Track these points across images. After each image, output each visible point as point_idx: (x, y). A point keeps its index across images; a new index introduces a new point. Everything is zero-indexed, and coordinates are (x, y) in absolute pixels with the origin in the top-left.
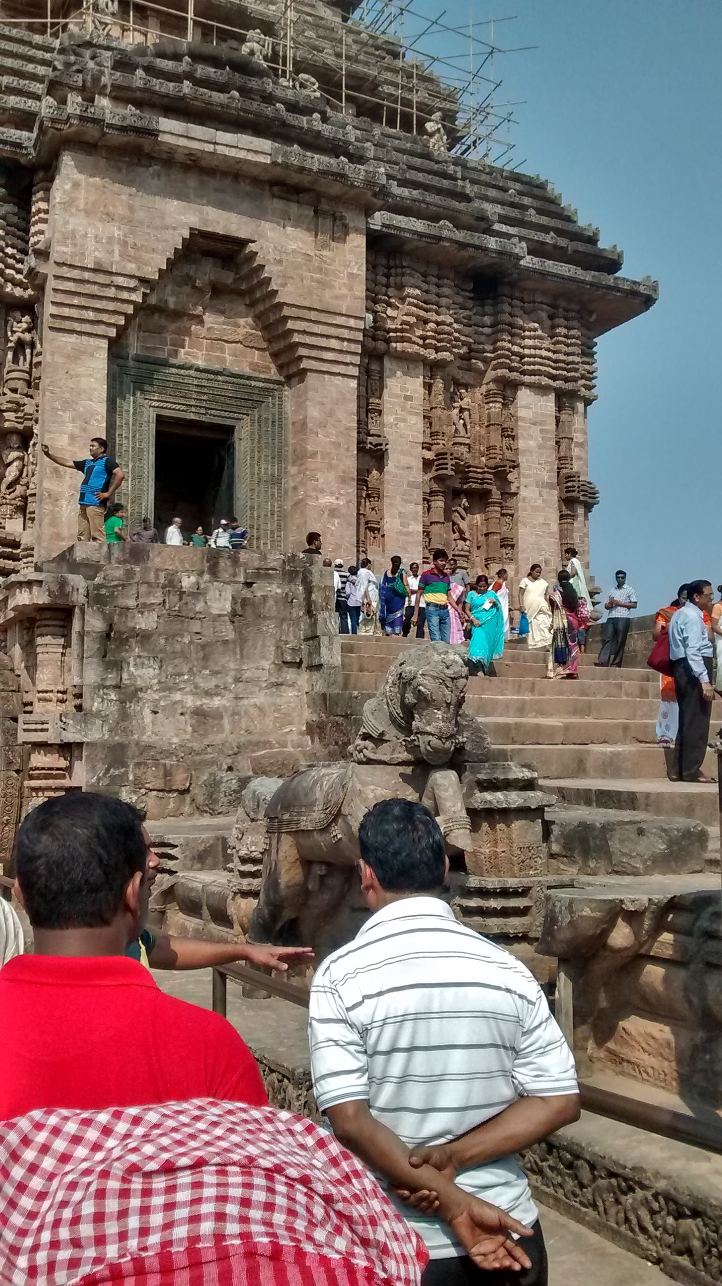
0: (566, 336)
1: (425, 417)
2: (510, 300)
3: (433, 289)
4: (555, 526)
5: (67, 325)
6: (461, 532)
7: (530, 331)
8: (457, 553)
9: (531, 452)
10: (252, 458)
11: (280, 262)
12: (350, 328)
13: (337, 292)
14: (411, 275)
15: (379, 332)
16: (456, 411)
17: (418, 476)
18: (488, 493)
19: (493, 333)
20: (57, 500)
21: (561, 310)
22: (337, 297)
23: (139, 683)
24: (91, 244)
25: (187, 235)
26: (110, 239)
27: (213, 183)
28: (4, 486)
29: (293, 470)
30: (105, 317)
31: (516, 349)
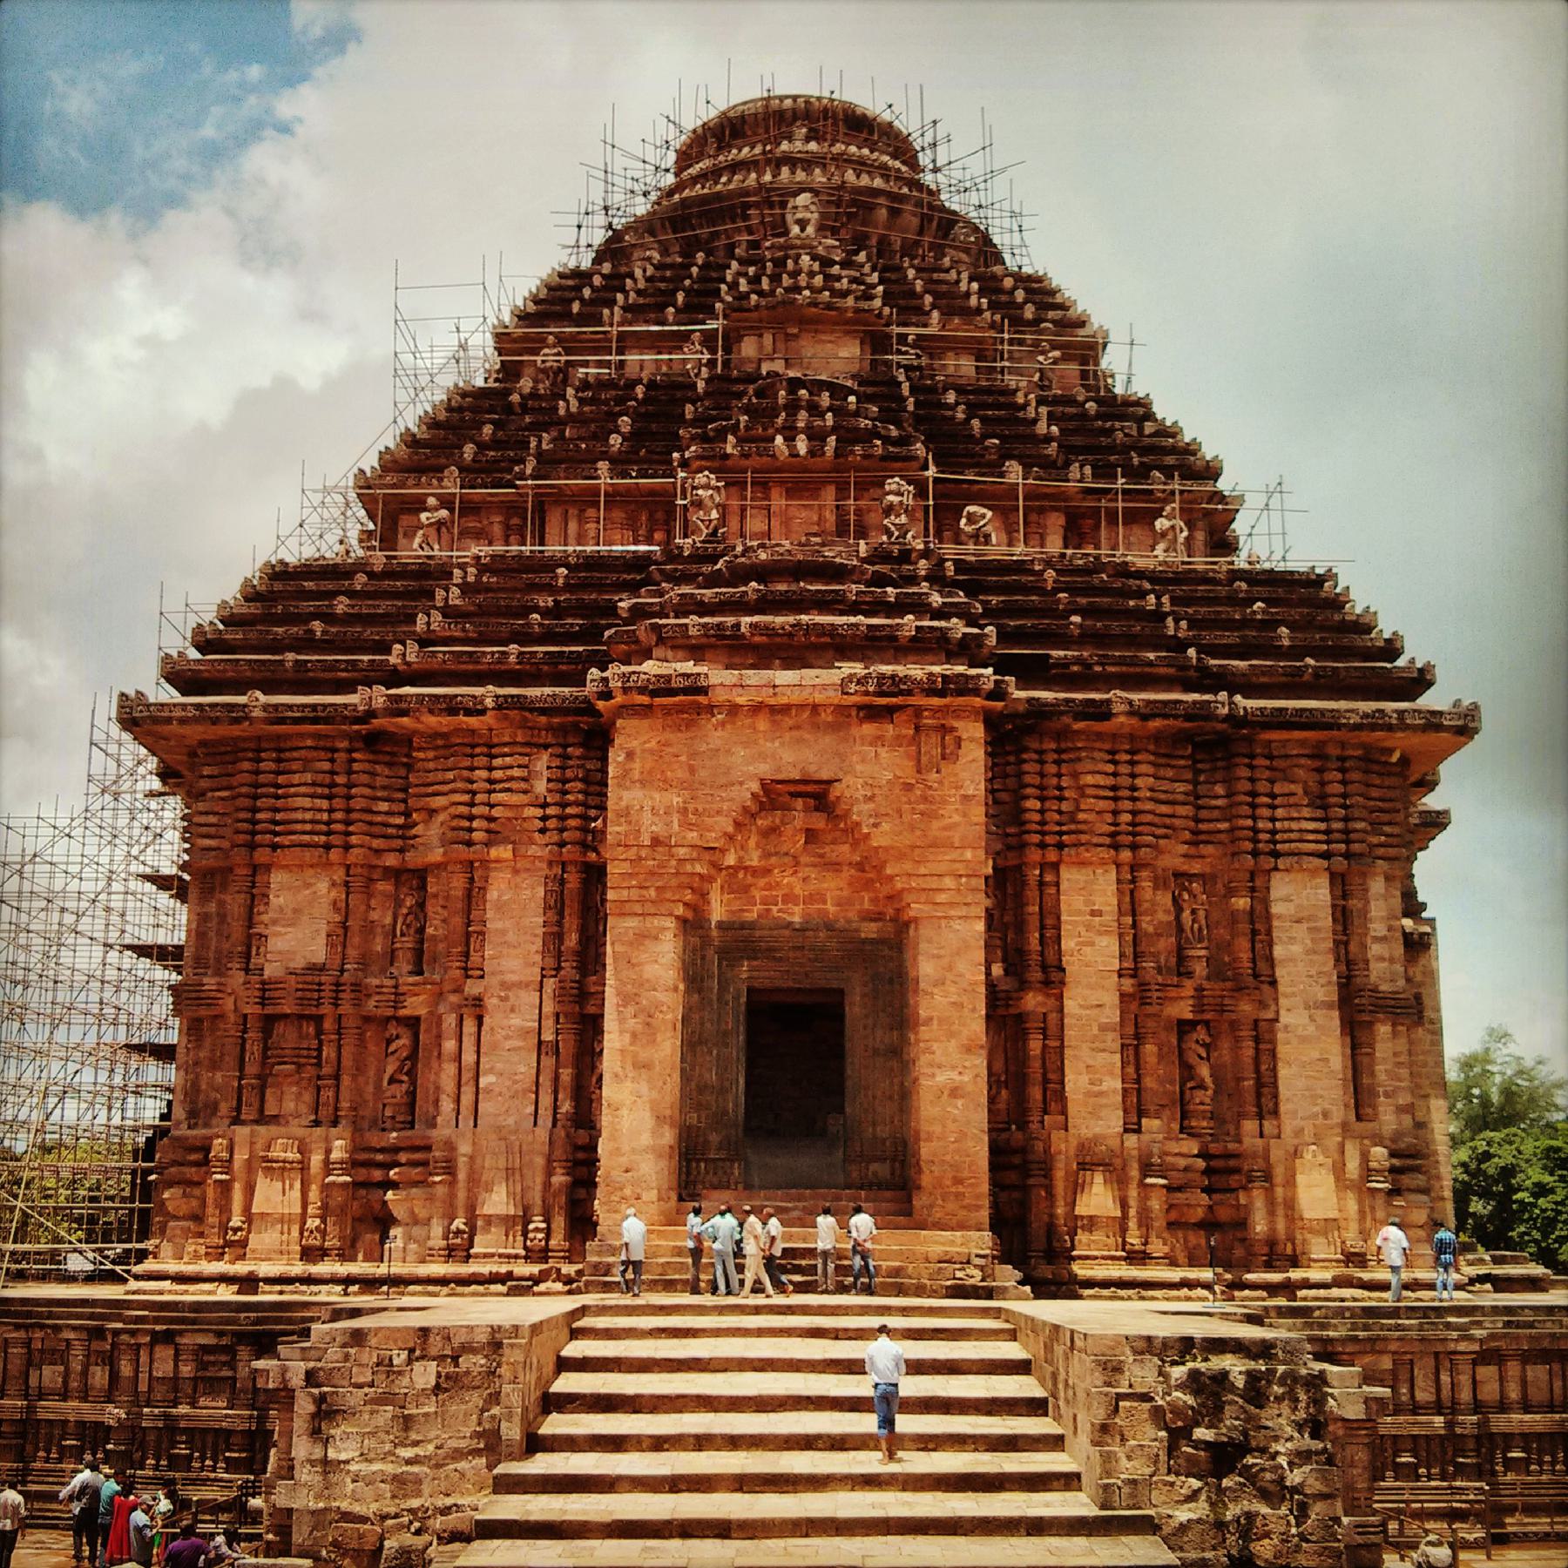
1: (1121, 936)
2: (1247, 761)
3: (1125, 769)
6: (1203, 1080)
8: (1192, 1107)
9: (1292, 960)
10: (865, 1027)
11: (871, 799)
17: (1112, 1015)
18: (1234, 1025)
19: (1231, 806)
22: (945, 829)
23: (343, 1457)
24: (647, 818)
25: (755, 786)
28: (594, 1080)
29: (912, 1037)
30: (668, 895)
31: (1260, 825)
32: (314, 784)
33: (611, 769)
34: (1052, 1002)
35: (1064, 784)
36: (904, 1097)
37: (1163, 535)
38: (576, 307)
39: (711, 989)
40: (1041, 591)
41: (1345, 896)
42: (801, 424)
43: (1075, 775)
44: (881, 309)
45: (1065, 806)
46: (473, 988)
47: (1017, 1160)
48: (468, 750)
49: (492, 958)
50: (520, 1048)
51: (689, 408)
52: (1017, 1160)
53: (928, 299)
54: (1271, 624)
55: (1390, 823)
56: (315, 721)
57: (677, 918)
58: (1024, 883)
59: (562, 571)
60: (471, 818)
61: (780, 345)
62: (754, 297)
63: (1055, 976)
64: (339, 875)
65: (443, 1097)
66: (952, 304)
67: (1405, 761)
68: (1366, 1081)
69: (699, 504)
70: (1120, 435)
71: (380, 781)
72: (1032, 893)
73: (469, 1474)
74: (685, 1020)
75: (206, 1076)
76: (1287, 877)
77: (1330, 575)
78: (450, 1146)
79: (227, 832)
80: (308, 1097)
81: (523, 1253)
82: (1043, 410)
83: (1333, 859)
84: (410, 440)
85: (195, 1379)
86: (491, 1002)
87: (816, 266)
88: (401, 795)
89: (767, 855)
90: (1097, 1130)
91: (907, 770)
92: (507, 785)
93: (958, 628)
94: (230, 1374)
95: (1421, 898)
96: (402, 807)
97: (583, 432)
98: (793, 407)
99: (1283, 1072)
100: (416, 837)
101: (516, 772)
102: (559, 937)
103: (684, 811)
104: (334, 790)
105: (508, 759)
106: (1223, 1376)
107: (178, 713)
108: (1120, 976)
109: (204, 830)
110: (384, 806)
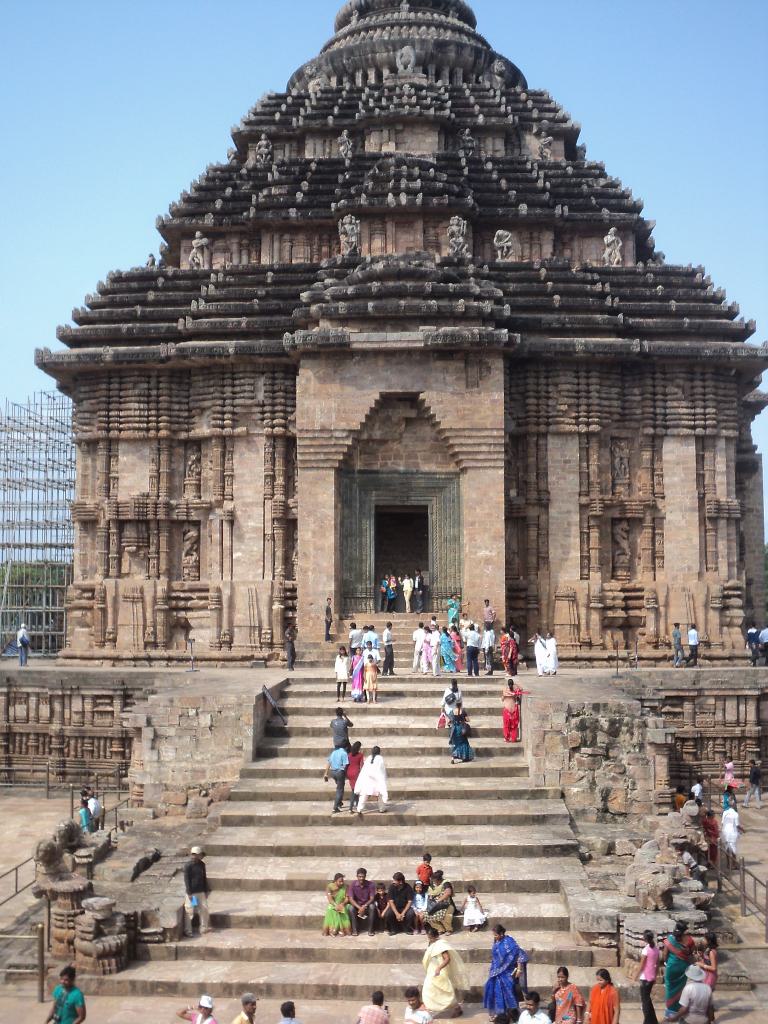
0: (704, 394)
3: (583, 381)
4: (696, 541)
5: (309, 465)
6: (624, 549)
7: (670, 394)
9: (674, 485)
12: (494, 437)
13: (482, 414)
14: (565, 375)
15: (541, 420)
16: (617, 460)
18: (641, 520)
19: (643, 400)
20: (305, 572)
21: (698, 376)
23: (167, 759)
25: (377, 397)
26: (329, 412)
27: (394, 360)
30: (331, 457)
31: (658, 411)
32: (139, 396)
33: (298, 388)
34: (543, 509)
35: (550, 390)
36: (458, 564)
37: (609, 245)
38: (277, 116)
39: (356, 507)
40: (537, 280)
41: (703, 449)
42: (403, 186)
43: (556, 385)
44: (450, 117)
45: (551, 402)
46: (228, 505)
47: (523, 595)
48: (221, 376)
49: (238, 489)
50: (254, 538)
51: (340, 177)
52: (523, 595)
53: (477, 108)
54: (666, 298)
55: (728, 409)
56: (139, 362)
57: (338, 471)
58: (528, 444)
59: (270, 274)
60: (223, 413)
61: (393, 137)
62: (377, 110)
63: (542, 497)
64: (155, 445)
65: (214, 564)
66: (490, 110)
67: (739, 374)
68: (710, 549)
69: (345, 233)
70: (585, 187)
71: (175, 392)
72: (532, 450)
73: (229, 767)
75: (89, 552)
76: (672, 440)
77: (701, 270)
78: (219, 590)
79: (95, 422)
81: (258, 645)
82: (542, 173)
83: (698, 430)
84: (187, 199)
85: (93, 712)
86: (238, 513)
87: (413, 91)
88: (186, 400)
90: (566, 578)
92: (242, 395)
93: (488, 306)
94: (109, 709)
95: (754, 443)
96: (186, 407)
97: (284, 190)
98: (398, 177)
99: (667, 546)
100: (194, 423)
101: (247, 388)
102: (273, 478)
104: (151, 399)
105: (242, 381)
106: (597, 721)
107: (66, 360)
108: (580, 495)
109: (83, 421)
110: (176, 407)
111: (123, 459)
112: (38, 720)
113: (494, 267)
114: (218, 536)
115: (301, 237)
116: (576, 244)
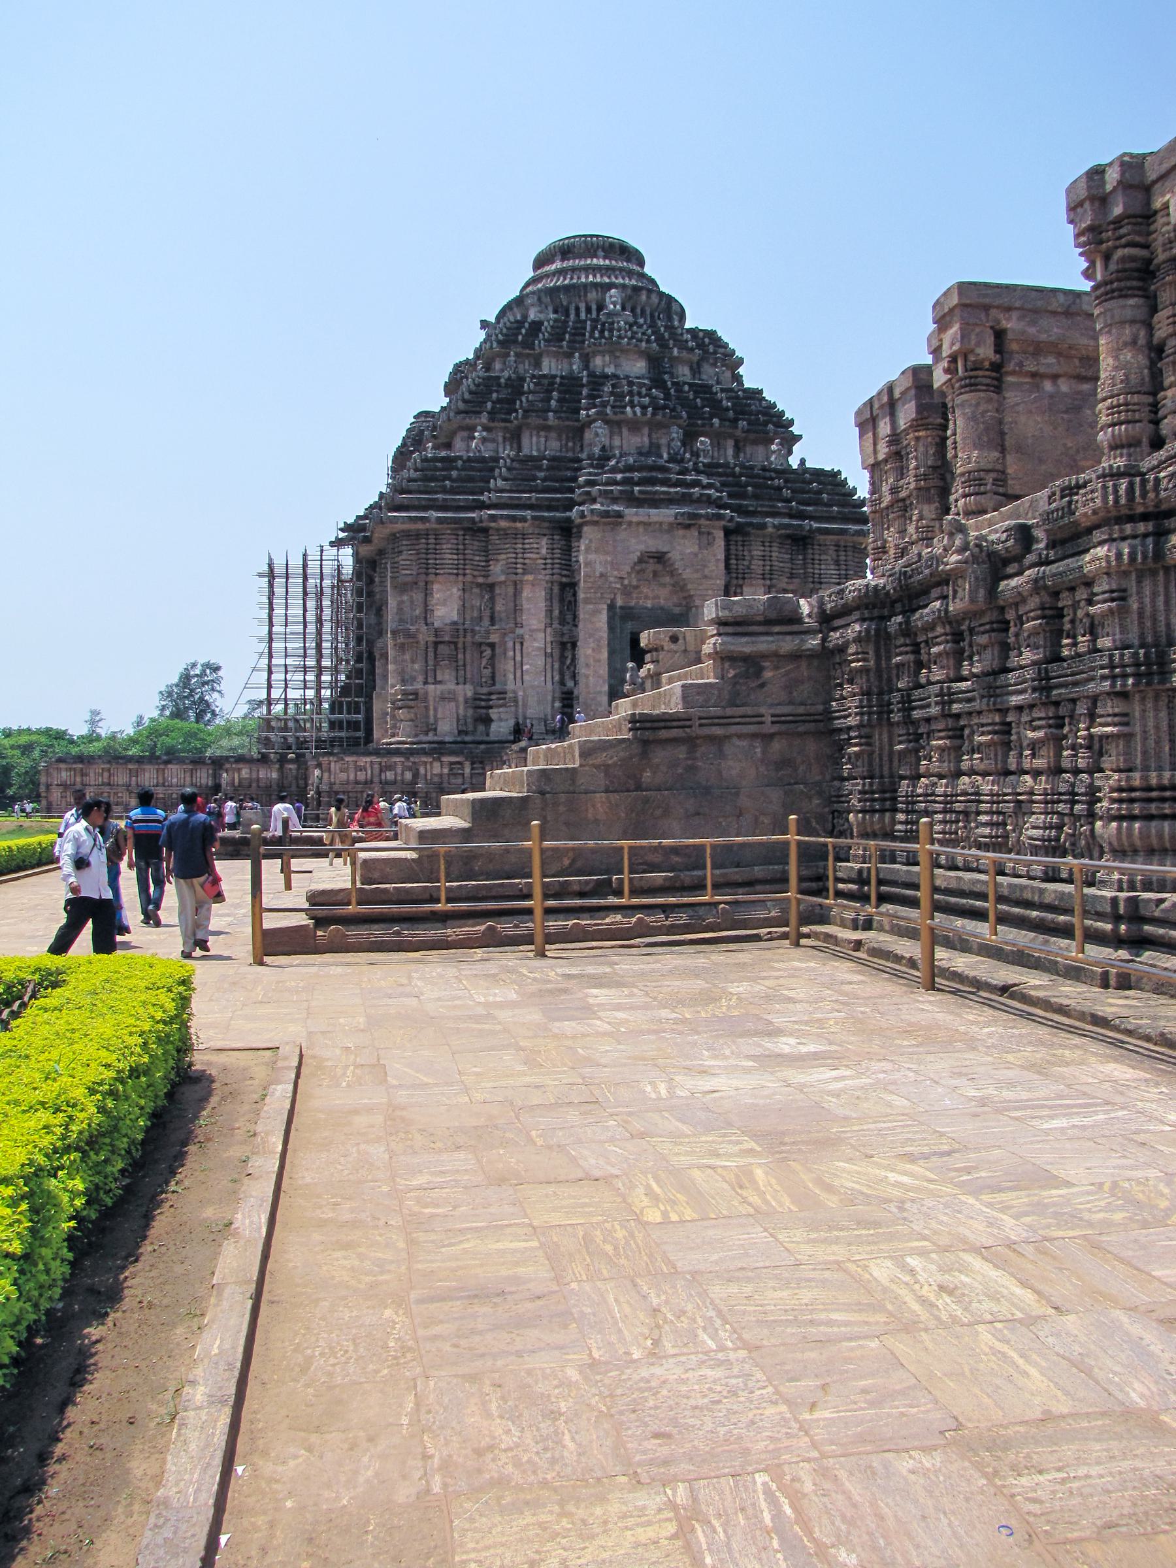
25: (638, 554)
26: (606, 562)
38: (520, 338)
40: (733, 475)
43: (750, 551)
46: (519, 631)
53: (671, 342)
54: (820, 492)
64: (461, 586)
70: (753, 407)
74: (609, 644)
77: (839, 472)
78: (515, 692)
80: (454, 674)
86: (527, 637)
89: (639, 580)
91: (695, 549)
103: (612, 563)
110: (477, 558)
111: (437, 596)
112: (403, 781)
113: (704, 465)
114: (511, 653)
115: (553, 435)
116: (749, 449)
